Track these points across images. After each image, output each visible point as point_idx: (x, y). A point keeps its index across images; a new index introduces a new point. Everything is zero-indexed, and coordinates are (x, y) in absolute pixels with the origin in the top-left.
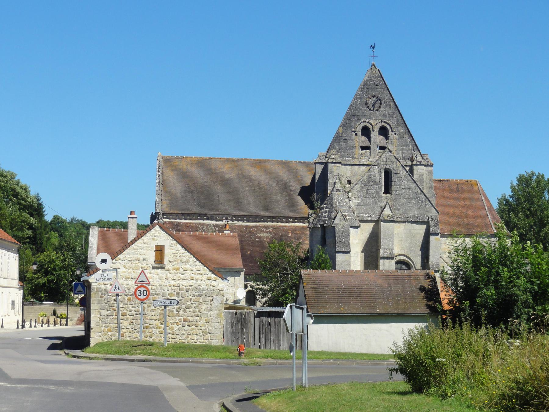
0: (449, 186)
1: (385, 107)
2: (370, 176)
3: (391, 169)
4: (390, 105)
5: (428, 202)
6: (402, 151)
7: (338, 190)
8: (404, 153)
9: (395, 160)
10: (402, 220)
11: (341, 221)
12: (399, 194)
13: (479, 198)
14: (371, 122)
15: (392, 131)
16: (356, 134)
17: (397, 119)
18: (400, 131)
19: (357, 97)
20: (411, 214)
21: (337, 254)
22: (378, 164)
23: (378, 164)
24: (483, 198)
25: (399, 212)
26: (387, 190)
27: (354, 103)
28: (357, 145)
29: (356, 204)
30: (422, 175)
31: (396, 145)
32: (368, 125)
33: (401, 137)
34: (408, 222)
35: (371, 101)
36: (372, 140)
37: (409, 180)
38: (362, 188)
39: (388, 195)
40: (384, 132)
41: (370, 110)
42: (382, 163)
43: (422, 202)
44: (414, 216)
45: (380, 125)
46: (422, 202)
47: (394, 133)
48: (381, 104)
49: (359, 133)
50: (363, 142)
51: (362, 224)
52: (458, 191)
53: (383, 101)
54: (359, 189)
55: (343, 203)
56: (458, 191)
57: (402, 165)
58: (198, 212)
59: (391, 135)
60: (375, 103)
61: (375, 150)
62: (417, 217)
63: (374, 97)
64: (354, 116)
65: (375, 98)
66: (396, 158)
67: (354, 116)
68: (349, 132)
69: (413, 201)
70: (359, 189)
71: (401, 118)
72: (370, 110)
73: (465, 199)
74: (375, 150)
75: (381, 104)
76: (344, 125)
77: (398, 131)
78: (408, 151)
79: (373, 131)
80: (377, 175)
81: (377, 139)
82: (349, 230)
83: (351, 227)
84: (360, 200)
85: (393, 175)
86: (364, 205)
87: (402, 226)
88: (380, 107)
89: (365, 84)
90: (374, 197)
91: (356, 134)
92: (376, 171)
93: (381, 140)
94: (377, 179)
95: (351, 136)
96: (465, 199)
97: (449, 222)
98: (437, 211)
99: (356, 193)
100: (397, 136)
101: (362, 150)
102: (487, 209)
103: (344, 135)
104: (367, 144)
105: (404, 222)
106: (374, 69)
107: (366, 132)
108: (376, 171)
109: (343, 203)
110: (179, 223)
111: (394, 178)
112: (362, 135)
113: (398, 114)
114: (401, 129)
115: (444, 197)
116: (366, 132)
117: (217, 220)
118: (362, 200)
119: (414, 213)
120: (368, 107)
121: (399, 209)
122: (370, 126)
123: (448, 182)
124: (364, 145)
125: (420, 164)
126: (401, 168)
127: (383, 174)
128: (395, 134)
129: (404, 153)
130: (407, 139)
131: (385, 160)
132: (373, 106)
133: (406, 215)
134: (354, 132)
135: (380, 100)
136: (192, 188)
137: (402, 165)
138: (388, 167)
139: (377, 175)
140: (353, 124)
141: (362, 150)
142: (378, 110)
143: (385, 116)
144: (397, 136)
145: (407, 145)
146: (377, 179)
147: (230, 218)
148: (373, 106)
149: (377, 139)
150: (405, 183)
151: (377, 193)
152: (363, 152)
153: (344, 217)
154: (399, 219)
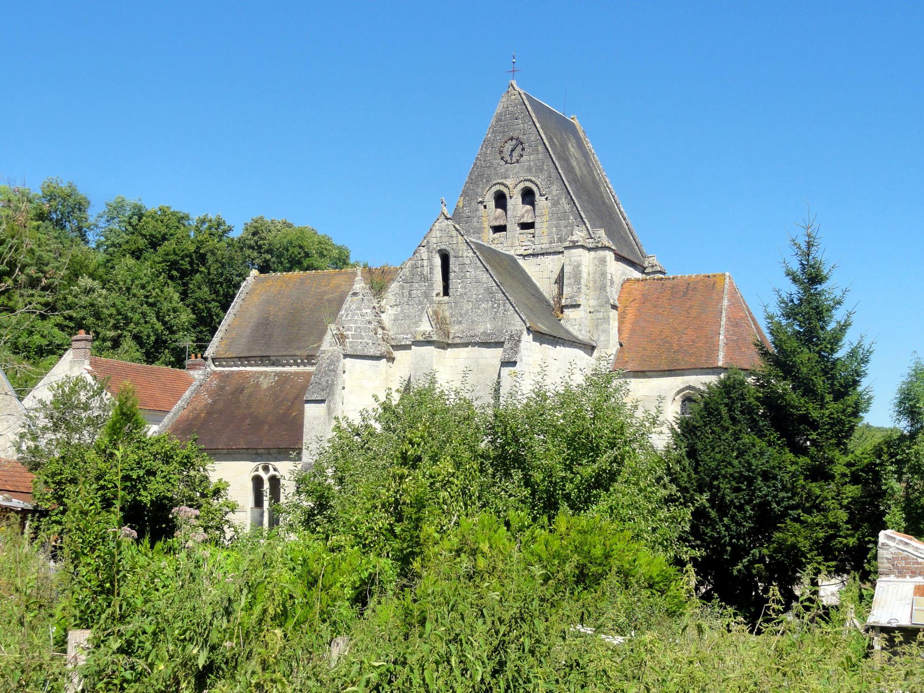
0: (672, 288)
1: (530, 154)
2: (415, 267)
3: (448, 249)
4: (537, 150)
5: (508, 305)
6: (557, 227)
7: (355, 294)
8: (561, 230)
9: (454, 233)
10: (462, 341)
11: (331, 346)
12: (461, 295)
13: (717, 305)
14: (508, 182)
15: (541, 195)
16: (485, 207)
17: (549, 173)
18: (554, 193)
19: (487, 143)
20: (480, 329)
21: (306, 405)
22: (428, 242)
23: (428, 242)
24: (725, 303)
25: (461, 327)
26: (446, 292)
27: (480, 154)
28: (486, 225)
29: (393, 317)
30: (579, 265)
31: (546, 218)
32: (502, 188)
33: (556, 203)
34: (474, 344)
35: (509, 146)
36: (509, 212)
37: (478, 268)
38: (402, 287)
39: (446, 297)
40: (528, 196)
41: (506, 162)
42: (434, 240)
43: (499, 305)
44: (484, 333)
45: (522, 186)
46: (499, 305)
47: (543, 198)
48: (523, 149)
49: (491, 204)
50: (496, 219)
51: (397, 354)
52: (685, 294)
53: (526, 145)
54: (397, 291)
55: (353, 315)
56: (685, 294)
57: (467, 242)
58: (259, 354)
59: (540, 201)
60: (512, 151)
61: (513, 229)
62: (489, 335)
63: (512, 139)
64: (481, 176)
65: (514, 142)
66: (457, 230)
67: (481, 176)
68: (474, 203)
69: (483, 305)
70: (397, 291)
71: (555, 171)
72: (506, 162)
73: (691, 307)
74: (513, 229)
75: (523, 149)
76: (465, 194)
77: (550, 193)
78: (566, 227)
79: (511, 197)
80: (425, 263)
81: (517, 208)
82: (338, 360)
83: (346, 356)
84: (399, 309)
85: (452, 260)
86: (404, 319)
87: (463, 352)
88: (522, 156)
89: (499, 120)
90: (420, 303)
91: (485, 207)
92: (425, 256)
93: (527, 211)
94: (426, 270)
95: (477, 210)
96: (691, 307)
97: (645, 349)
98: (524, 321)
99: (393, 298)
100: (549, 203)
101: (494, 233)
102: (723, 323)
103: (467, 210)
104: (501, 222)
105: (466, 345)
106: (513, 92)
107: (501, 200)
108: (425, 256)
109: (353, 315)
110: (232, 372)
111: (453, 265)
112: (497, 206)
113: (551, 163)
114: (555, 189)
115: (655, 307)
116: (501, 200)
117: (284, 366)
118: (402, 310)
119: (485, 327)
120: (502, 158)
121: (460, 323)
122: (505, 190)
123: (675, 281)
124: (497, 224)
125: (574, 246)
126: (465, 247)
127: (438, 261)
128: (547, 199)
129: (561, 230)
130: (567, 207)
131: (438, 234)
132: (511, 155)
133: (472, 333)
134: (481, 202)
135: (522, 143)
136: (271, 318)
137: (467, 242)
138: (443, 247)
139: (425, 263)
140: (479, 190)
141: (494, 233)
142: (518, 161)
143: (529, 170)
144: (549, 203)
145: (564, 216)
146: (426, 270)
147: (299, 361)
148: (511, 155)
149: (517, 208)
150: (471, 273)
151: (426, 295)
152: (497, 235)
153: (341, 338)
154: (458, 341)
